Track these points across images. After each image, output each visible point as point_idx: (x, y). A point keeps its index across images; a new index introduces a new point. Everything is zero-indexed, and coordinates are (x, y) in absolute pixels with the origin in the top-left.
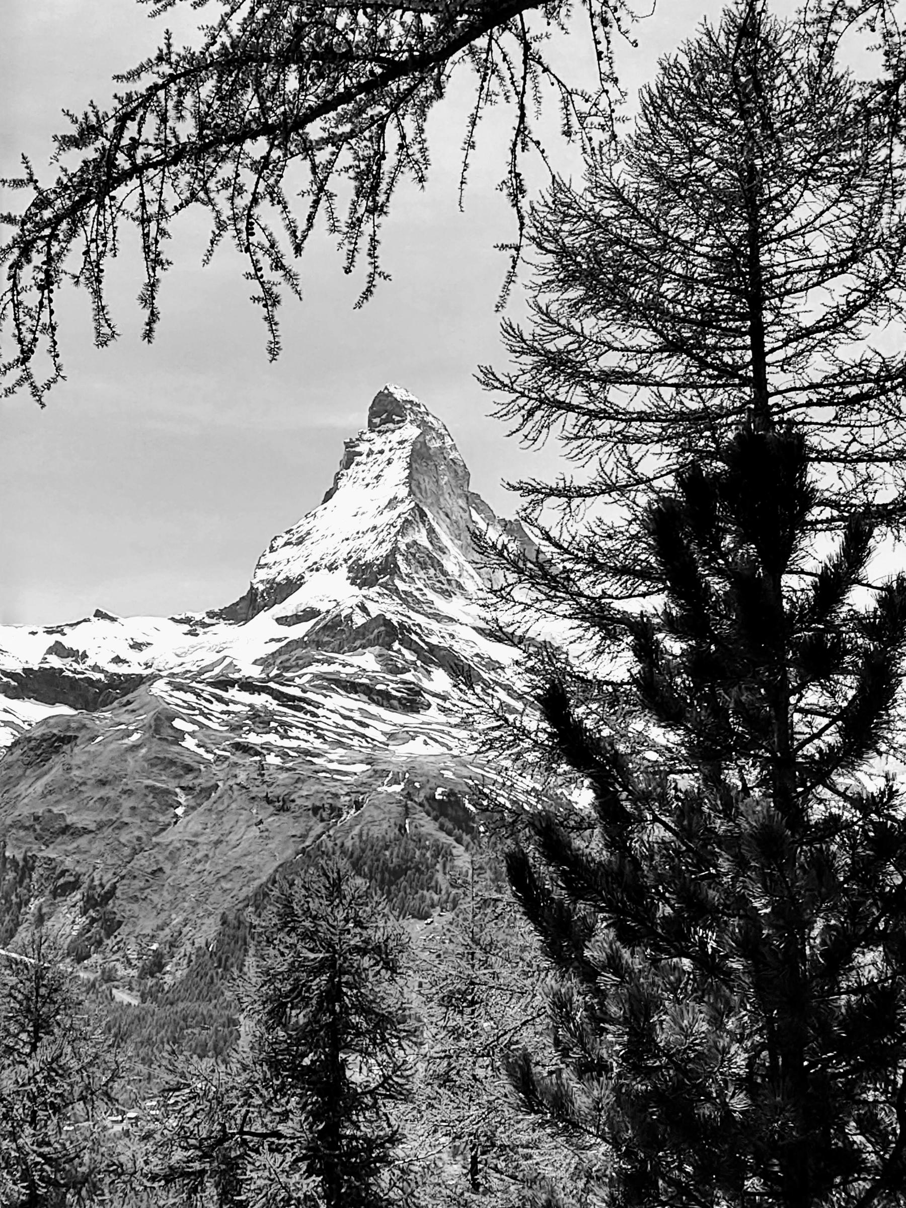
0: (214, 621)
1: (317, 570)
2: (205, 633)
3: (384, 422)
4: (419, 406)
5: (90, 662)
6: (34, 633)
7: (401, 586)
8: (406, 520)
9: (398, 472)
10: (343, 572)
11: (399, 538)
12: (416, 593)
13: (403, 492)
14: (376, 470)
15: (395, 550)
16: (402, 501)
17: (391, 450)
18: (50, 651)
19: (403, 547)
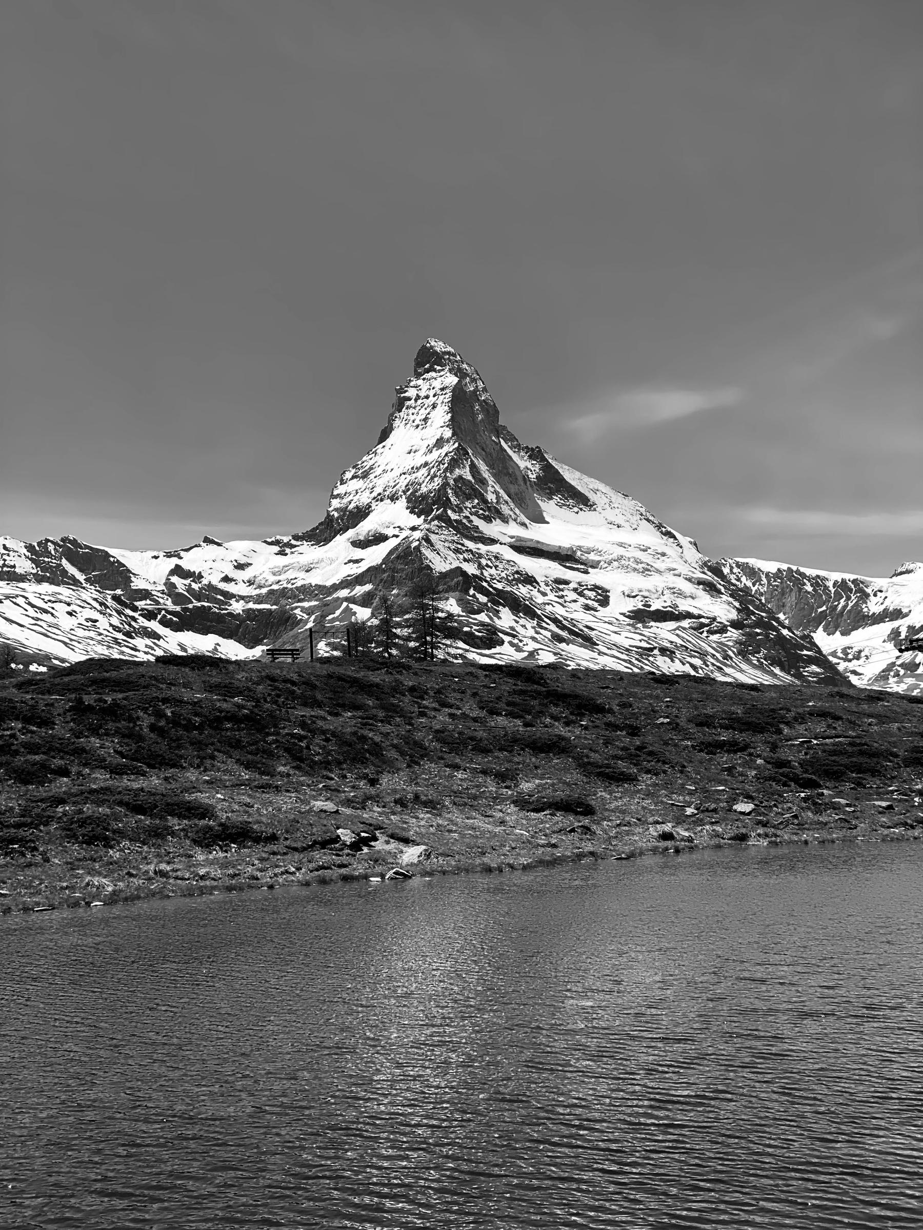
0: (299, 543)
1: (382, 500)
2: (292, 553)
3: (428, 371)
4: (454, 355)
5: (205, 581)
6: (156, 557)
7: (453, 516)
8: (453, 459)
9: (441, 416)
10: (402, 503)
11: (448, 474)
12: (464, 521)
13: (448, 433)
14: (423, 413)
15: (445, 485)
16: (448, 441)
17: (434, 396)
18: (173, 572)
19: (452, 482)
